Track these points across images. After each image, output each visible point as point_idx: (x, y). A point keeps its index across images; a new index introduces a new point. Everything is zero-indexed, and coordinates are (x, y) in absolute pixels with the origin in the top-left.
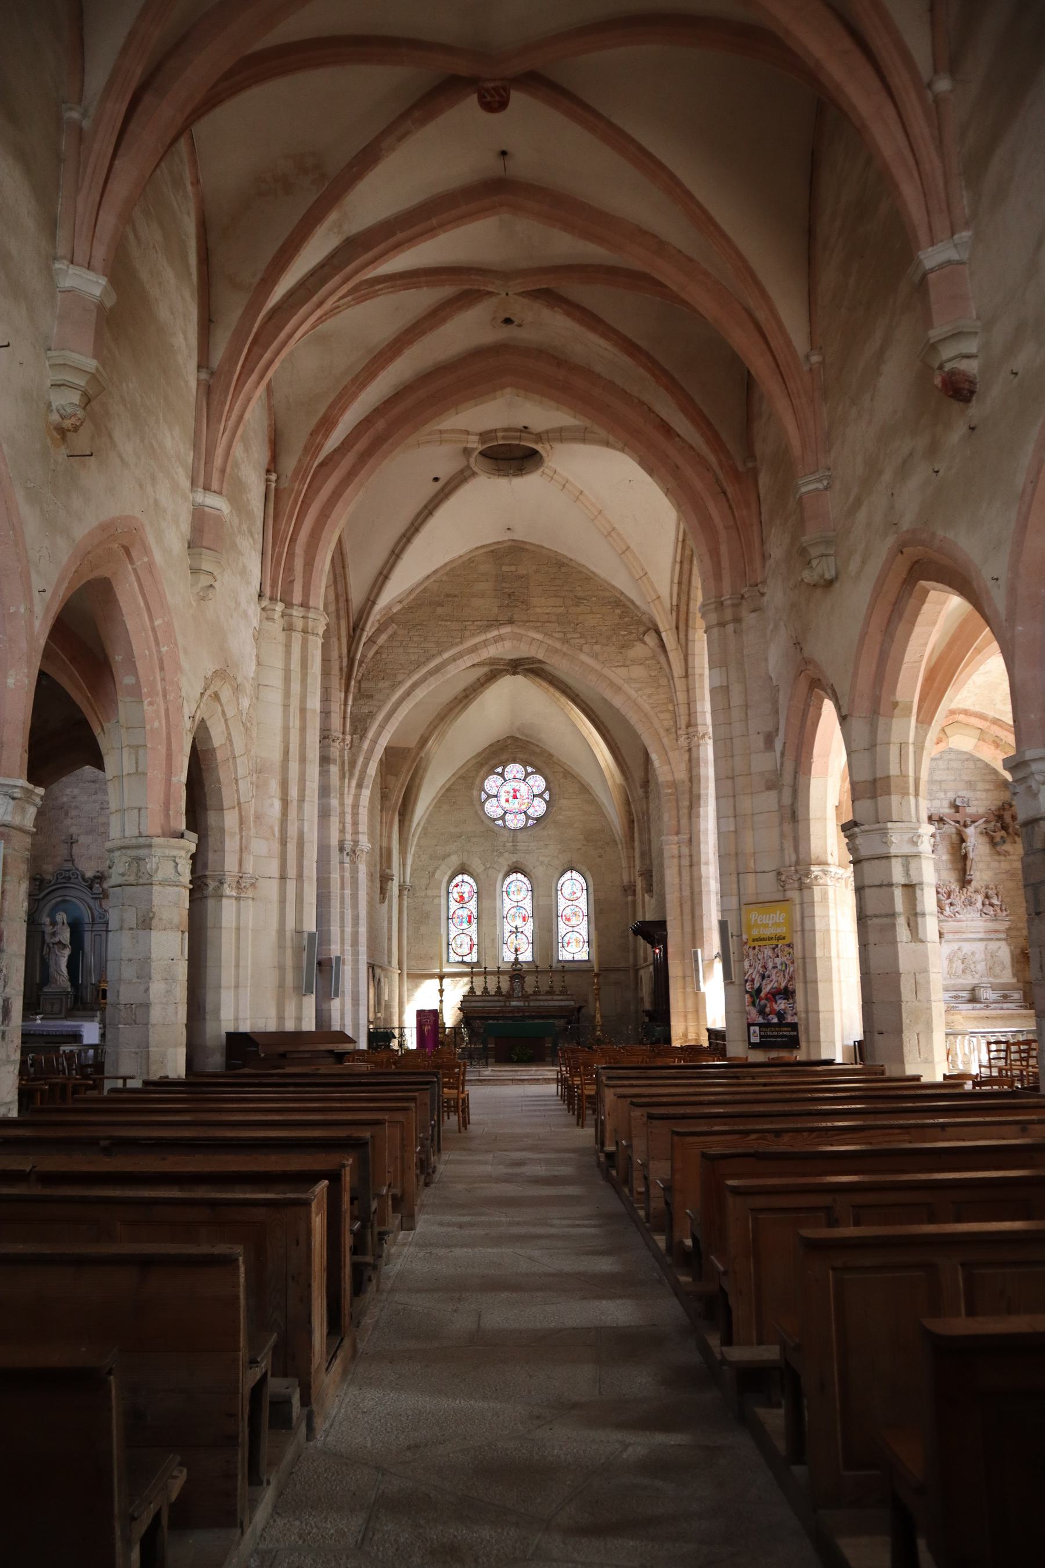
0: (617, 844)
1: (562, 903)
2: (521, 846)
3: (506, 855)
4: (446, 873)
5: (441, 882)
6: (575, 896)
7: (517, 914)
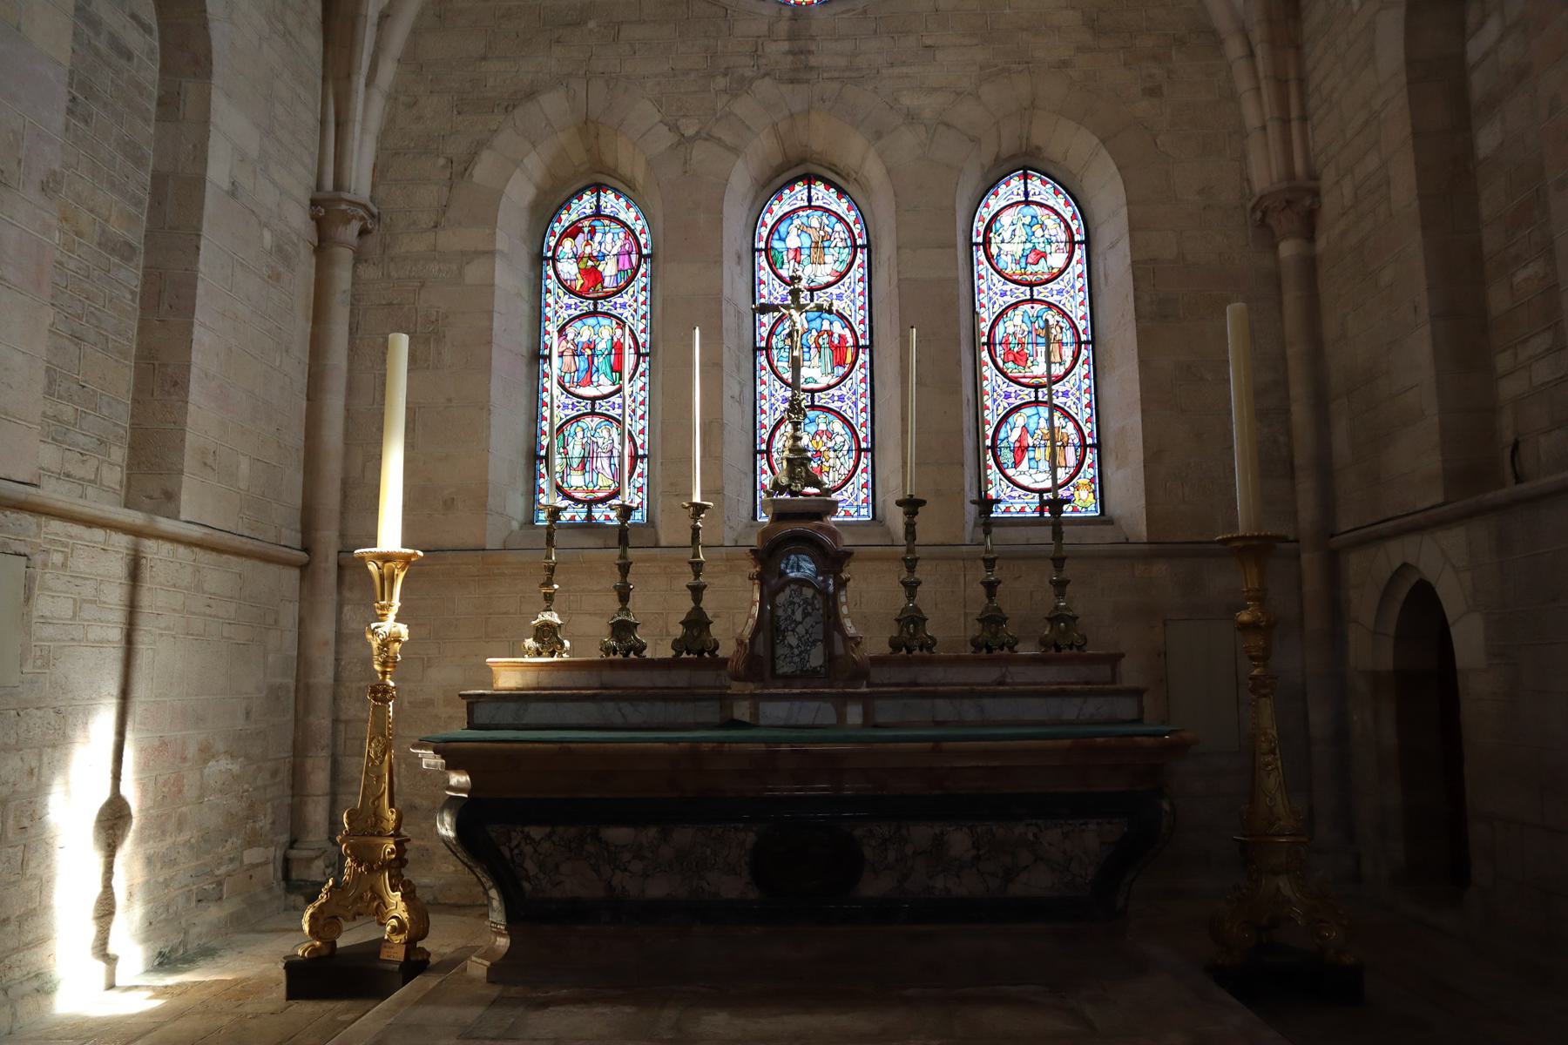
0: (1216, 42)
1: (992, 293)
3: (765, 87)
4: (518, 163)
5: (495, 197)
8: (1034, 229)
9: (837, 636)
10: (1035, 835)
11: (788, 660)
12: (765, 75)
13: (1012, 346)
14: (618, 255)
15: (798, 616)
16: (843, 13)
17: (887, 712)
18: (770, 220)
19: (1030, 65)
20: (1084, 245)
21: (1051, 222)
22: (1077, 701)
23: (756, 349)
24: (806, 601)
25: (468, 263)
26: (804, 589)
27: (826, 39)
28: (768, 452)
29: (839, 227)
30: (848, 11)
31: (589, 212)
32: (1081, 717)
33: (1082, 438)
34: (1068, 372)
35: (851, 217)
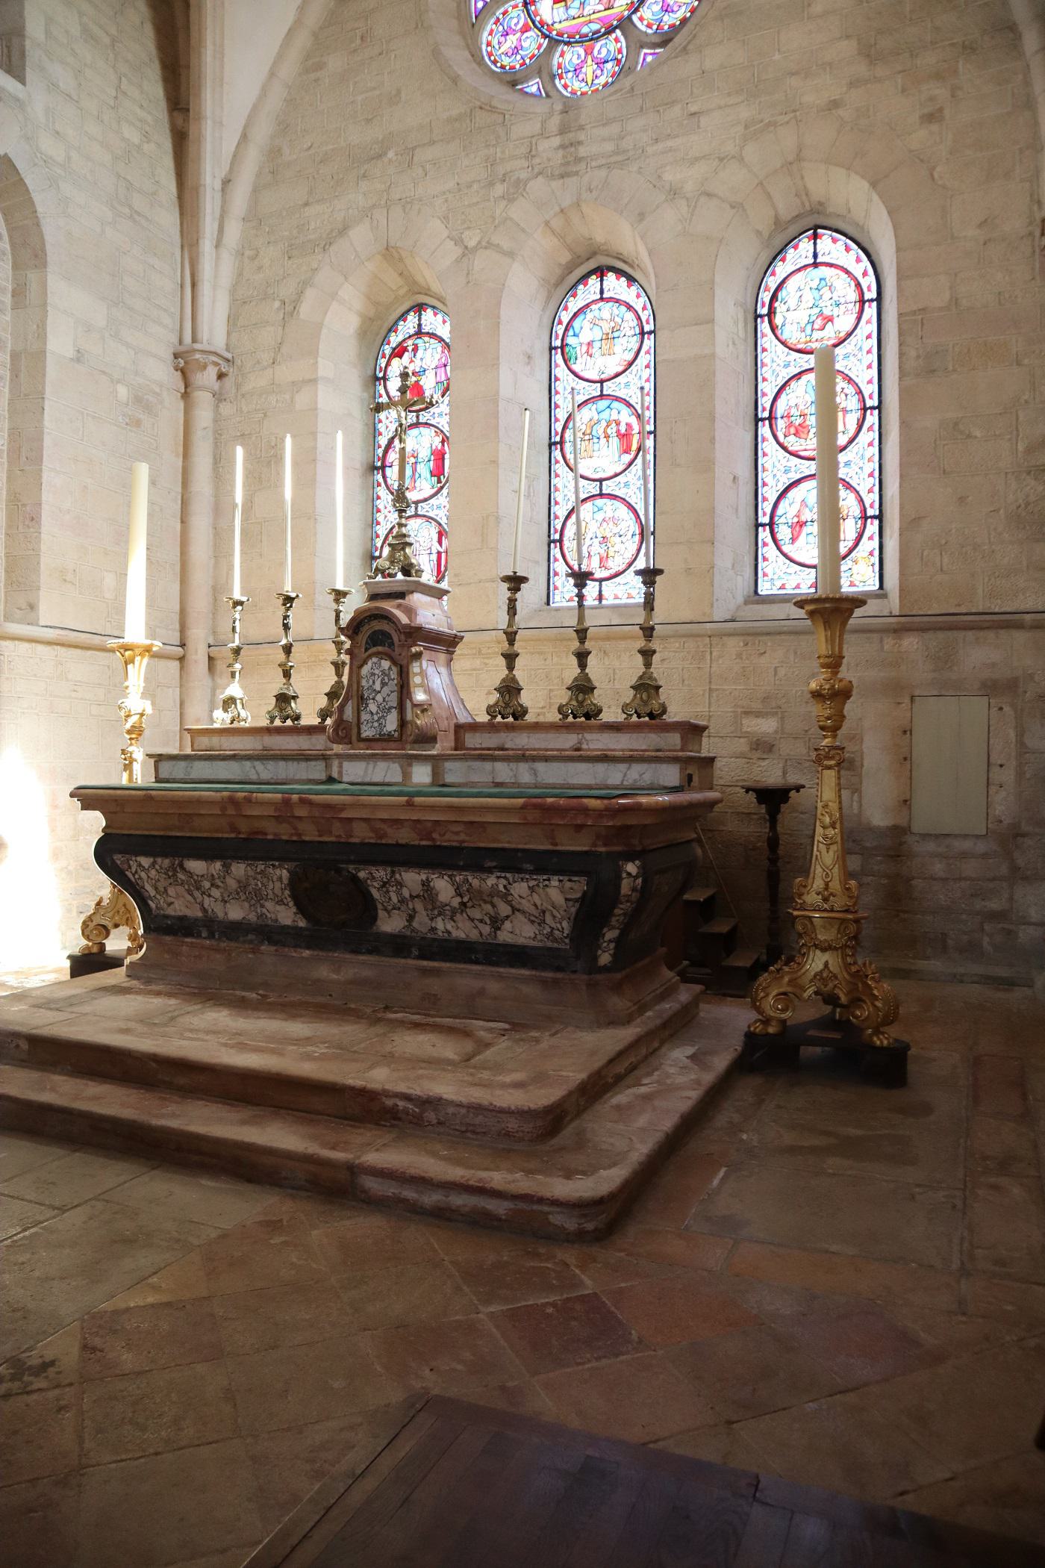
2: (595, 143)
6: (830, 334)
7: (599, 430)
8: (821, 293)
9: (409, 704)
10: (505, 887)
11: (369, 725)
12: (540, 173)
13: (793, 419)
14: (436, 368)
15: (377, 687)
16: (610, 95)
17: (455, 772)
18: (565, 317)
19: (798, 113)
20: (875, 303)
21: (842, 282)
22: (622, 767)
23: (551, 444)
24: (383, 672)
25: (297, 392)
26: (383, 661)
27: (594, 127)
28: (561, 541)
29: (630, 315)
30: (616, 92)
31: (412, 331)
32: (625, 783)
33: (864, 510)
34: (851, 441)
35: (638, 305)
